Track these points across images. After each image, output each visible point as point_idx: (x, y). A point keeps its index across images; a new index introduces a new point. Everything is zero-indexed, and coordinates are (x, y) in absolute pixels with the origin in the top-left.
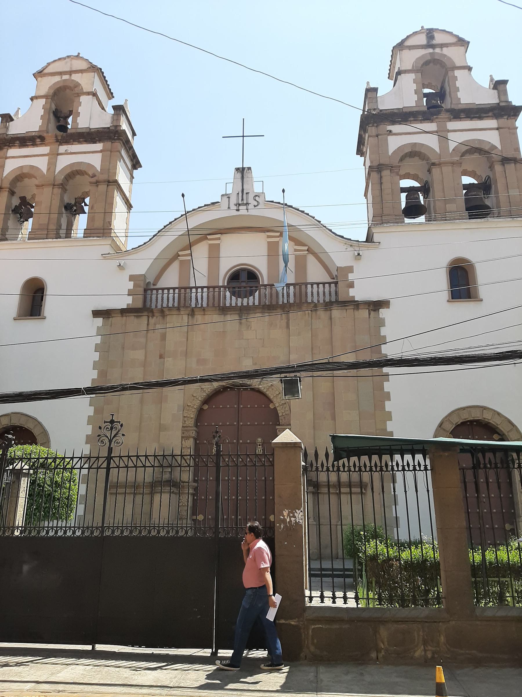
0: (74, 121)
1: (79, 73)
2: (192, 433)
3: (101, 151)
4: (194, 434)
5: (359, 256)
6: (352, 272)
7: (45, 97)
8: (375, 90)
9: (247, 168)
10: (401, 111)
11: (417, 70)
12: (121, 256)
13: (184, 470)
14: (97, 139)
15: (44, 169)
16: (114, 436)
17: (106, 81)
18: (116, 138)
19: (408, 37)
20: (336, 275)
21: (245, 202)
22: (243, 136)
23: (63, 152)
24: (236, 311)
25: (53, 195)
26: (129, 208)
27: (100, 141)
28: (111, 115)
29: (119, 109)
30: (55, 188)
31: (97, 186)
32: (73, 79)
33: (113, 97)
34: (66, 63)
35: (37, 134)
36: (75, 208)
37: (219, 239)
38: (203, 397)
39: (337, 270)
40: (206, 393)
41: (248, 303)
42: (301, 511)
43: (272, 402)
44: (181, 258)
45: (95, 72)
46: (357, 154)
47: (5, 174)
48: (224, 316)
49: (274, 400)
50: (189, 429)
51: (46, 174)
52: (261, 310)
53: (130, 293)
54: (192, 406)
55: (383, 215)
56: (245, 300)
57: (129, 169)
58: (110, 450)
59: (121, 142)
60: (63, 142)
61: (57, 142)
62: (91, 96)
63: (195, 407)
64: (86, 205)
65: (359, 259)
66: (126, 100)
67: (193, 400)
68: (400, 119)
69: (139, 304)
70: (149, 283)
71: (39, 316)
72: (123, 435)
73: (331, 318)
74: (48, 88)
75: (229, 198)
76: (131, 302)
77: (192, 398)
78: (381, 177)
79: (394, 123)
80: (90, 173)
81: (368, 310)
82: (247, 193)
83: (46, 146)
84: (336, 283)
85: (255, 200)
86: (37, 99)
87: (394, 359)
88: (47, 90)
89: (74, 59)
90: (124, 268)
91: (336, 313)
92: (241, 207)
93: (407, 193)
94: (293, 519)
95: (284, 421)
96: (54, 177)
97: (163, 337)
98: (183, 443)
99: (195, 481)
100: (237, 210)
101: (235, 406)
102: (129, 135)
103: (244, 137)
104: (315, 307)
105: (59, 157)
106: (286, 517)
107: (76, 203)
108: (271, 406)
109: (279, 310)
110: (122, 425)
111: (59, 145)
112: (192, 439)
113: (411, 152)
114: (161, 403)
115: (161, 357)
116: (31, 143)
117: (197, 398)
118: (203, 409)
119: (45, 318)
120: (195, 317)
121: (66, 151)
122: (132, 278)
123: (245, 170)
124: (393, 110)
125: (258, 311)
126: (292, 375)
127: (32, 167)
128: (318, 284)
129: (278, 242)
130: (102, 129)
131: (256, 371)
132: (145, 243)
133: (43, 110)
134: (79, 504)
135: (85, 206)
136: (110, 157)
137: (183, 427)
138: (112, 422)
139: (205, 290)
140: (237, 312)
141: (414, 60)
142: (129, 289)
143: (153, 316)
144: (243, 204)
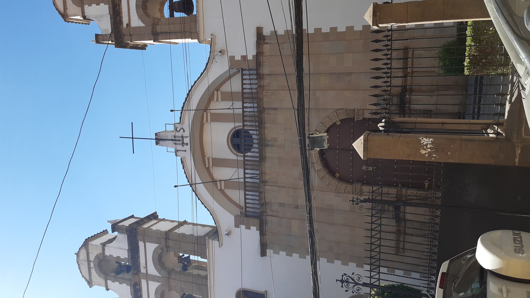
0: (123, 260)
1: (89, 255)
4: (359, 185)
8: (97, 36)
9: (155, 136)
10: (112, 16)
11: (82, 3)
12: (221, 233)
14: (136, 245)
15: (157, 284)
16: (353, 280)
17: (95, 235)
18: (135, 232)
19: (57, 9)
20: (236, 69)
21: (181, 139)
22: (133, 138)
23: (145, 270)
26: (186, 223)
27: (137, 243)
28: (119, 234)
29: (115, 227)
32: (93, 260)
33: (107, 230)
34: (82, 263)
35: (132, 288)
36: (186, 263)
37: (208, 158)
38: (329, 177)
39: (233, 69)
40: (326, 175)
41: (257, 139)
42: (422, 139)
43: (335, 122)
44: (223, 188)
45: (88, 244)
46: (145, 49)
49: (334, 121)
51: (160, 283)
53: (248, 228)
54: (336, 186)
55: (190, 32)
56: (255, 141)
57: (158, 222)
58: (365, 285)
59: (138, 228)
61: (138, 274)
62: (106, 248)
63: (337, 183)
64: (183, 255)
65: (224, 51)
66: (108, 222)
67: (331, 185)
68: (119, 17)
69: (257, 221)
71: (264, 295)
72: (353, 274)
73: (270, 75)
74: (100, 278)
75: (178, 151)
76: (255, 227)
78: (162, 33)
79: (121, 22)
80: (160, 251)
81: (264, 45)
82: (175, 137)
83: (141, 282)
84: (243, 70)
85: (180, 130)
86: (108, 286)
87: (296, 60)
88: (101, 279)
89: (79, 257)
90: (229, 231)
91: (265, 70)
93: (174, 12)
94: (429, 146)
96: (163, 277)
97: (282, 205)
99: (397, 186)
100: (187, 145)
101: (338, 151)
102: (132, 221)
103: (133, 137)
104: (260, 87)
105: (149, 273)
106: (427, 152)
107: (182, 263)
108: (339, 123)
109: (262, 116)
110: (345, 274)
111: (141, 273)
112: (362, 187)
113: (143, 9)
115: (297, 207)
116: (139, 292)
117: (330, 182)
118: (339, 177)
119: (266, 291)
122: (237, 225)
123: (158, 137)
124: (112, 23)
126: (307, 141)
127: (156, 293)
128: (243, 84)
130: (129, 242)
131: (303, 169)
132: (211, 215)
134: (411, 276)
135: (184, 256)
137: (353, 194)
138: (342, 281)
139: (246, 171)
141: (75, 5)
142: (246, 229)
144: (183, 140)
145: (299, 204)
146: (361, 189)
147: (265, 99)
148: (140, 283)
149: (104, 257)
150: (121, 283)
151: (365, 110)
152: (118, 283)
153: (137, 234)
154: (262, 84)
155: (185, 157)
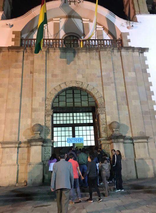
2: (51, 113)
5: (132, 27)
6: (129, 35)
24: (72, 50)
37: (59, 20)
48: (66, 53)
52: (85, 50)
53: (13, 40)
63: (52, 99)
69: (19, 45)
70: (23, 38)
73: (121, 56)
91: (124, 52)
92: (71, 3)
95: (101, 106)
97: (33, 63)
109: (94, 51)
114: (32, 97)
115: (31, 73)
120: (50, 54)
122: (14, 33)
125: (83, 51)
129: (88, 24)
137: (45, 109)
140: (73, 51)
143: (26, 52)
144: (72, 2)
145: (34, 74)
147: (105, 52)
151: (105, 115)
154: (115, 51)
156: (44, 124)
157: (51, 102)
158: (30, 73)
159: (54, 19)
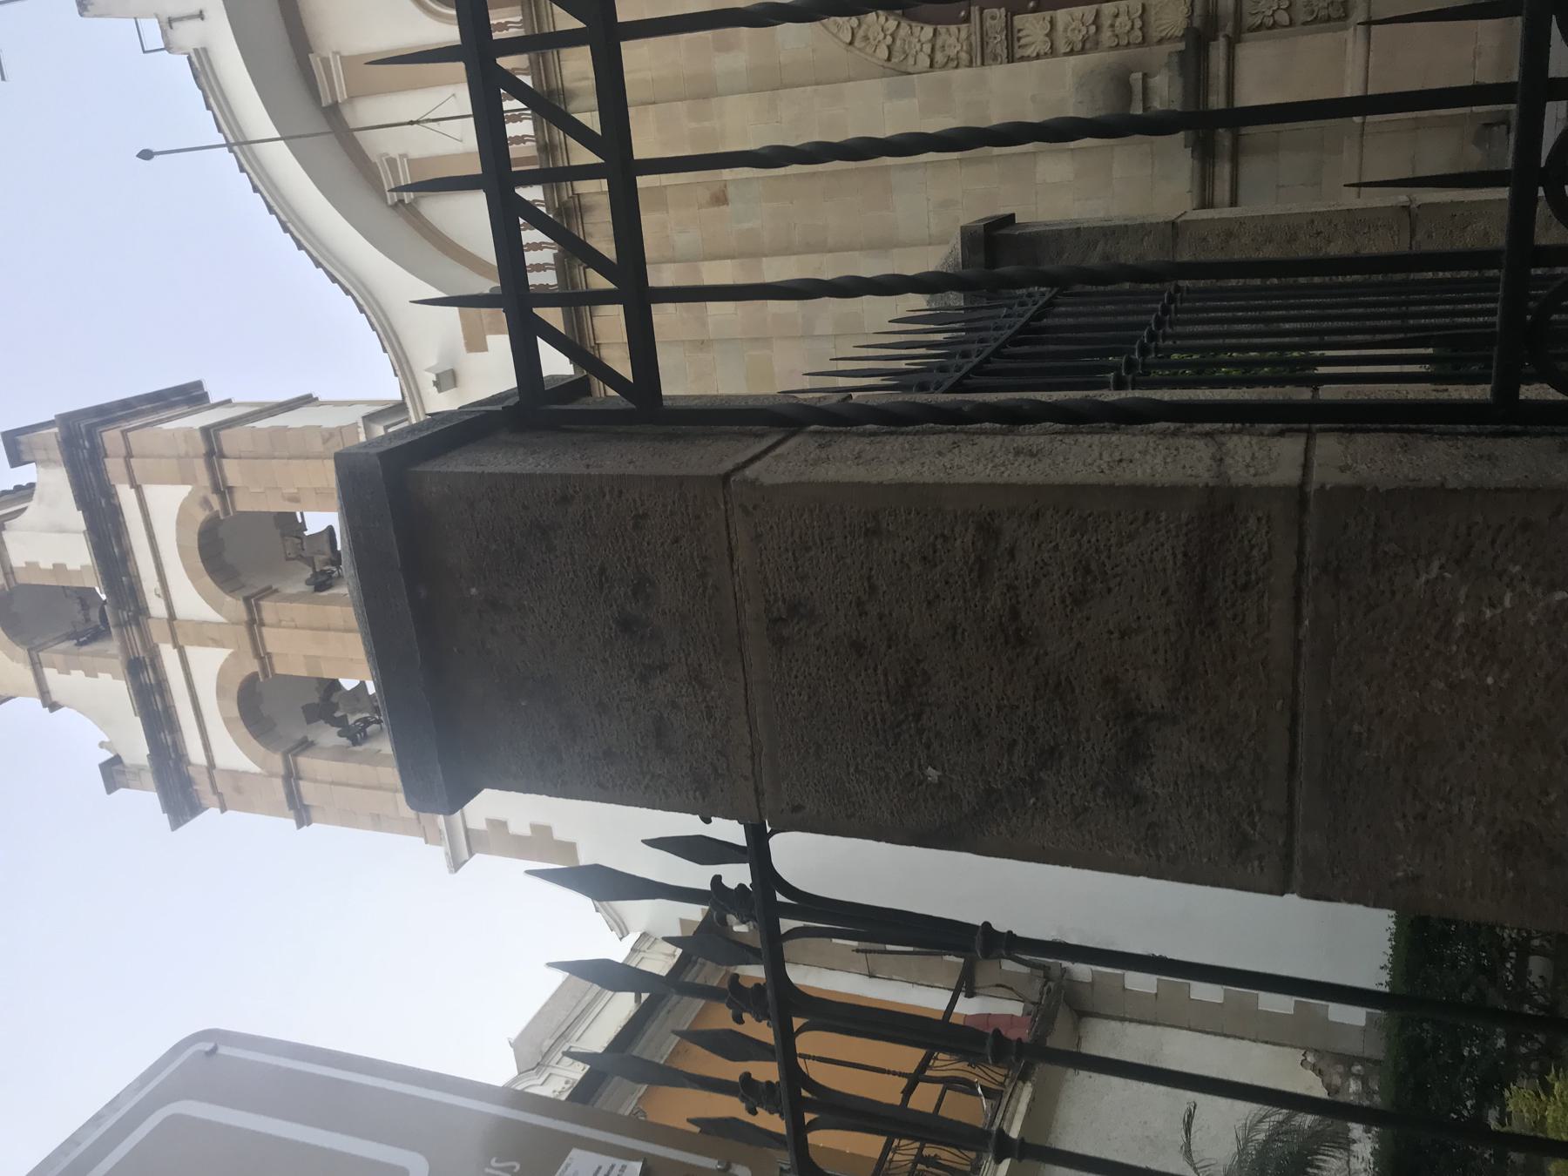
2: (993, 18)
3: (138, 489)
7: (36, 667)
13: (1141, 29)
25: (283, 623)
26: (309, 402)
27: (110, 494)
28: (42, 470)
30: (261, 619)
31: (230, 489)
47: (255, 768)
50: (975, 39)
51: (229, 651)
60: (137, 606)
61: (138, 625)
63: (892, 24)
75: (170, 21)
77: (863, 44)
80: (201, 515)
86: (48, 692)
90: (445, 372)
96: (233, 623)
98: (1035, 54)
105: (182, 611)
111: (150, 617)
112: (1016, 18)
116: (158, 698)
121: (159, 596)
133: (72, 672)
136: (144, 456)
137: (970, 64)
146: (1009, 27)
148: (156, 661)
149: (5, 574)
150: (91, 673)
152: (81, 673)
153: (103, 455)
155: (205, 50)
156: (1072, 59)
157: (917, 30)
158: (723, 208)
159: (326, 100)
